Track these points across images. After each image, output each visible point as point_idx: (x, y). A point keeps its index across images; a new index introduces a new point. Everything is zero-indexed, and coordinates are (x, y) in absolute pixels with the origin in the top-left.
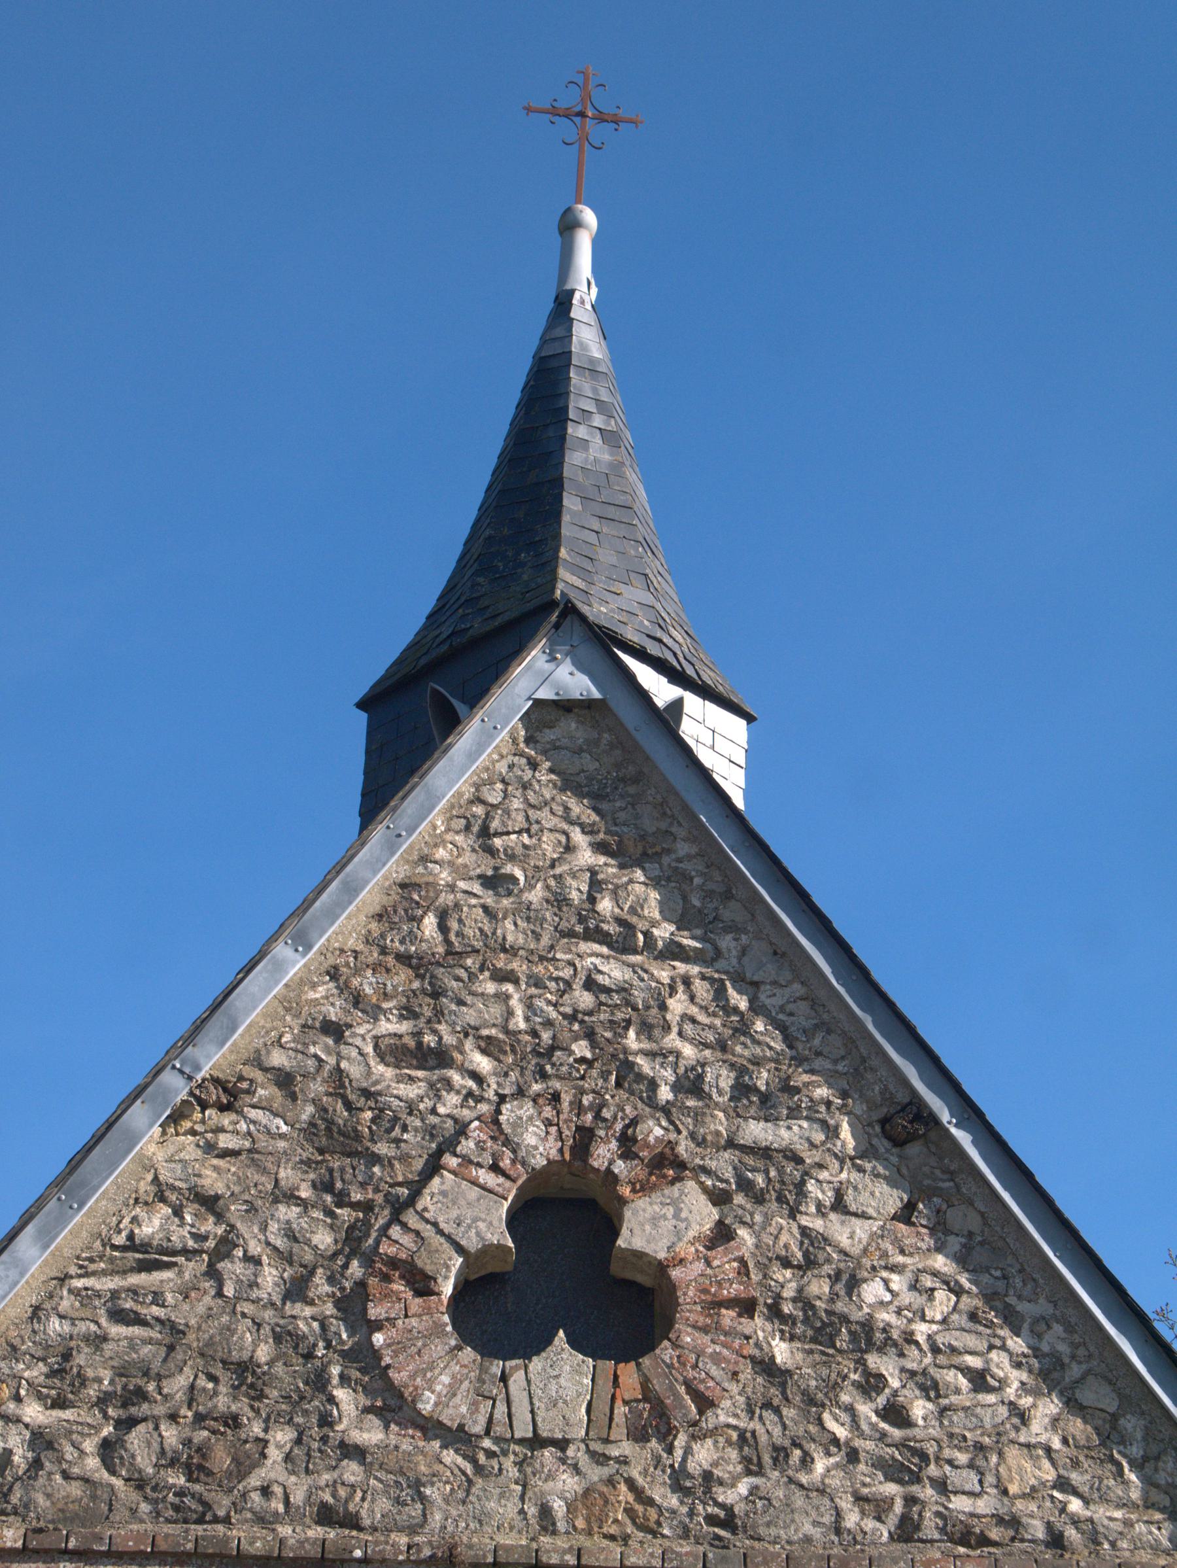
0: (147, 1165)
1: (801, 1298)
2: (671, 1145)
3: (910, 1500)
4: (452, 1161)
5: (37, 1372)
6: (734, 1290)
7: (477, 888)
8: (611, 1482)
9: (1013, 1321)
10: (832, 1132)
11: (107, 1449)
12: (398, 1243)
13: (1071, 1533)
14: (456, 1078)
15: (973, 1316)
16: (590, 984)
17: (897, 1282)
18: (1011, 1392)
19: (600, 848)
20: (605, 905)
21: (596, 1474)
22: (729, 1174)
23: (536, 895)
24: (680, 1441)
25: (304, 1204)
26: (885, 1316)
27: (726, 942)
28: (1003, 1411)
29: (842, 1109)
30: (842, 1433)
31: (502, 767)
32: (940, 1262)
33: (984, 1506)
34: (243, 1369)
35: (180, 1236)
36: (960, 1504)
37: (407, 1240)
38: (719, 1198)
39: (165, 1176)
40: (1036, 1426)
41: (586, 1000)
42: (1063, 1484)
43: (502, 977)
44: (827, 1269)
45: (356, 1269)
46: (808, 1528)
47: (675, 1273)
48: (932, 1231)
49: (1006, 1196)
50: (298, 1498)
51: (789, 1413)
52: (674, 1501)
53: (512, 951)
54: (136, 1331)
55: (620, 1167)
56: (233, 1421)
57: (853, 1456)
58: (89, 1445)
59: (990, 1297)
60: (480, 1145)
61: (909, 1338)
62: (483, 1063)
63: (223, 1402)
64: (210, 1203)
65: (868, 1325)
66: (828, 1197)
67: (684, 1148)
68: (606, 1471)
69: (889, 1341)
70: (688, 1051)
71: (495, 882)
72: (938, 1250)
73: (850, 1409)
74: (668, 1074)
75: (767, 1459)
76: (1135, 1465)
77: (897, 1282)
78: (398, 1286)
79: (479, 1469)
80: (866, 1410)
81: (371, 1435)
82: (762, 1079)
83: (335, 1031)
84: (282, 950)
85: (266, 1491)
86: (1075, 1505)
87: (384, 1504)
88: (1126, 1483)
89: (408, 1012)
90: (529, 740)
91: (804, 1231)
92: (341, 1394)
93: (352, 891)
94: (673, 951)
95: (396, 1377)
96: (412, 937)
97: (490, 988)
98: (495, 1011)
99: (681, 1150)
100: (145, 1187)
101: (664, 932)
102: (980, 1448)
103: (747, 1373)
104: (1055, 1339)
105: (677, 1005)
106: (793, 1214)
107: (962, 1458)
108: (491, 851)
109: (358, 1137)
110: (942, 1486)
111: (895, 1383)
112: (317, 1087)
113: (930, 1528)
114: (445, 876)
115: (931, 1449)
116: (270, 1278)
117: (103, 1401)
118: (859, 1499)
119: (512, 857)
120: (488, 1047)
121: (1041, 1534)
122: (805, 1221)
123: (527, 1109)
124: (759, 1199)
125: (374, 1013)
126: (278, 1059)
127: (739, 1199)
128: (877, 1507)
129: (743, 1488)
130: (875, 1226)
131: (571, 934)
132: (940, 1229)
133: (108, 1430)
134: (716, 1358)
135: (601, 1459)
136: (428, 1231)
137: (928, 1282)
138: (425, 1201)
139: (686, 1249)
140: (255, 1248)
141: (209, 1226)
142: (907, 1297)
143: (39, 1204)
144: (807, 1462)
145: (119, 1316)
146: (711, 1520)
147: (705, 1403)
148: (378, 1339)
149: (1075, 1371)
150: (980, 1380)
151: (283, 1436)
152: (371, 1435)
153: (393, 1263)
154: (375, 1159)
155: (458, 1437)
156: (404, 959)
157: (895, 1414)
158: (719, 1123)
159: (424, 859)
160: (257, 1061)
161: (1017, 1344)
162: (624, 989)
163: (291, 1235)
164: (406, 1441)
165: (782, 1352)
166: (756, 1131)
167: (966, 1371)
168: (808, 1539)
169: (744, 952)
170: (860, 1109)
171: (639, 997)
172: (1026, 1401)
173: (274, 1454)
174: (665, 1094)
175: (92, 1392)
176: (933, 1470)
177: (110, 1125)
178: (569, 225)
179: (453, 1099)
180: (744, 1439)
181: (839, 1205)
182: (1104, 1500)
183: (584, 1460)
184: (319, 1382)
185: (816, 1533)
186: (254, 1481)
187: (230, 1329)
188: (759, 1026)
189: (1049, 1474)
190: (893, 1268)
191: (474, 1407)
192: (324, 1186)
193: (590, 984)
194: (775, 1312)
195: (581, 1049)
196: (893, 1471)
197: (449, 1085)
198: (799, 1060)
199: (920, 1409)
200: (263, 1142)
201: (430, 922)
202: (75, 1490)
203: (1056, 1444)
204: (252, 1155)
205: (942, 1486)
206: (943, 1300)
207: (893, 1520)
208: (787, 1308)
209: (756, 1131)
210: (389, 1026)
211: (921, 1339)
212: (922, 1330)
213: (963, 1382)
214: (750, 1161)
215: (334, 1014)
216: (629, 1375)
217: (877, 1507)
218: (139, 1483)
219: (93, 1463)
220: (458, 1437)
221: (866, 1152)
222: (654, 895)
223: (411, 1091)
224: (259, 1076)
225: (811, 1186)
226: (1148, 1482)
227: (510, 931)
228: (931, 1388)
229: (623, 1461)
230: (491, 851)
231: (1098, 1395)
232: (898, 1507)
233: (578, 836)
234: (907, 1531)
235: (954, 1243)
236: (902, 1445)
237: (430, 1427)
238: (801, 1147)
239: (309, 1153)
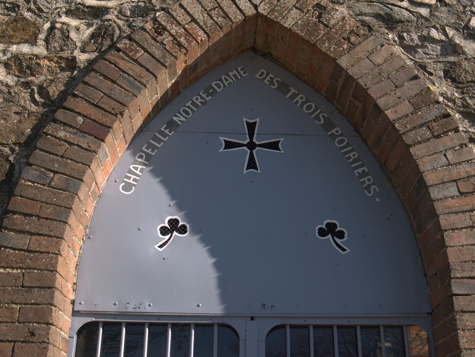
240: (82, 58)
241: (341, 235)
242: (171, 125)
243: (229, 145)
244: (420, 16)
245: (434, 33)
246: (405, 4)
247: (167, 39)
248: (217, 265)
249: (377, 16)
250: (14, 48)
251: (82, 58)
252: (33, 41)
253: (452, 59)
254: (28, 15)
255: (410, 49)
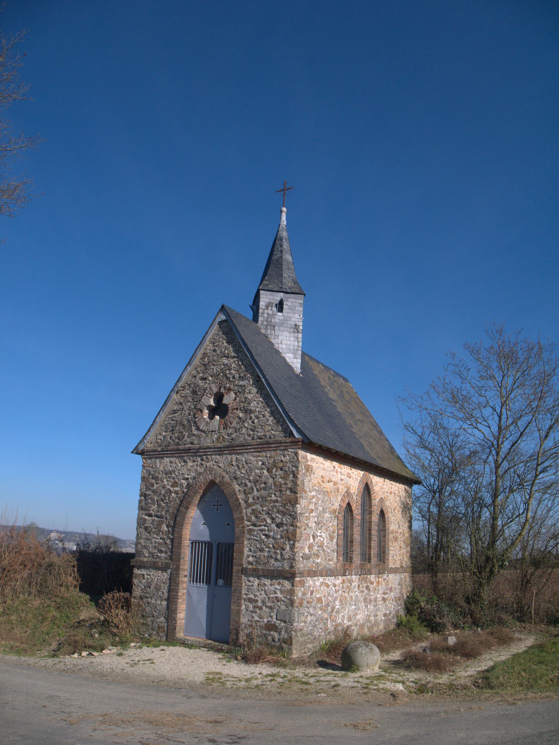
0: (175, 400)
1: (244, 407)
2: (230, 387)
3: (254, 434)
4: (205, 394)
5: (164, 428)
6: (235, 407)
7: (212, 352)
8: (220, 436)
9: (268, 406)
10: (249, 381)
11: (171, 437)
12: (199, 406)
13: (272, 436)
14: (207, 381)
15: (264, 407)
16: (224, 364)
17: (255, 403)
18: (267, 417)
19: (227, 342)
20: (226, 352)
21: (219, 435)
22: (237, 390)
23: (218, 352)
24: (228, 429)
25: (190, 402)
26: (253, 408)
27: (240, 354)
28: (266, 420)
29: (251, 378)
30: (246, 425)
31: (216, 333)
32: (261, 399)
33: (262, 434)
34: (183, 425)
35: (178, 409)
36: (259, 434)
37: (200, 406)
38: (236, 394)
39: (177, 401)
40: (269, 422)
41: (223, 366)
42: (272, 430)
43: (214, 365)
44: (247, 402)
45: (195, 410)
46: (242, 439)
47: (229, 406)
48: (260, 394)
49: (268, 388)
50: (188, 441)
51: (241, 423)
52: (227, 437)
53: (215, 361)
54: (174, 422)
55: (224, 391)
56: (182, 432)
57: (248, 429)
58: (169, 437)
59: (266, 403)
60: (208, 391)
61: (256, 411)
62: (210, 378)
63: (181, 430)
64: (181, 403)
65: (251, 410)
66: (248, 391)
67: (232, 387)
68: (219, 434)
69: (253, 412)
70: (234, 372)
71: (214, 351)
72: (261, 397)
73: (248, 422)
74: (231, 376)
75: (238, 430)
76: (281, 426)
77: (255, 403)
78: (199, 412)
79: (207, 436)
80: (250, 422)
81: (196, 432)
82: (242, 375)
83: (195, 377)
84: (188, 367)
85: (185, 441)
86: (273, 432)
87: (197, 441)
88: (279, 428)
89: (203, 373)
90: (220, 327)
91: (245, 397)
92: (193, 427)
93: (196, 357)
94: (234, 357)
95: (198, 424)
96: (204, 361)
97: (212, 367)
98: (212, 370)
99: (231, 387)
100: (175, 403)
101: (233, 354)
102: (262, 426)
103: (237, 419)
104: (274, 409)
105: (233, 365)
106: (244, 394)
107: (260, 427)
108: (214, 346)
109: (196, 392)
110: (257, 432)
111: (253, 418)
112: (192, 386)
113: (255, 437)
114: (208, 351)
115: (256, 426)
116: (187, 412)
117: (170, 431)
118: (248, 435)
119: (217, 346)
120: (212, 376)
121: (269, 437)
122: (245, 395)
123: (214, 385)
124: (240, 393)
125: (199, 373)
126: (189, 382)
127: (238, 394)
128: (249, 435)
129: (235, 435)
130: (253, 395)
131: (222, 357)
132: (261, 394)
133: (171, 435)
134: (233, 417)
135: (219, 433)
136: (202, 404)
137: (259, 402)
138: (202, 400)
139: (230, 402)
140: (185, 409)
141: (182, 407)
142: (256, 405)
143: (162, 407)
144: (242, 430)
145: (172, 420)
146: (231, 439)
147: (231, 424)
148: (196, 420)
149: (276, 412)
150: (264, 416)
151: (187, 434)
152: (196, 432)
153: (199, 409)
154: (198, 395)
155: (204, 432)
156: (203, 365)
157: (253, 422)
158: (237, 382)
159: (206, 349)
160: (186, 383)
161: (269, 410)
162: (227, 364)
163: (189, 407)
164: (199, 433)
165: (241, 415)
166: (241, 383)
167: (262, 415)
168: (241, 441)
169: (242, 355)
170: (253, 377)
171: (229, 365)
172: (268, 418)
173: (186, 436)
174: (231, 379)
175: (169, 430)
176: (256, 430)
177: (169, 395)
178: (281, 212)
179: (207, 384)
180: (235, 428)
181: (250, 393)
182: (277, 431)
183: (217, 433)
184: (191, 426)
185: (242, 440)
186: (184, 440)
187: (182, 420)
188: (242, 367)
189: (270, 428)
190: (254, 401)
191: (206, 428)
192: (193, 399)
193: (224, 364)
194: (241, 410)
195: (221, 374)
196: (253, 430)
197: (206, 382)
198: (247, 371)
199: (256, 421)
200: (187, 395)
201: (207, 358)
202: (167, 443)
203: (272, 424)
204: (186, 397)
205: (257, 432)
206: (261, 404)
207: (251, 437)
208: (242, 409)
209: (241, 383)
210: (201, 375)
211: (257, 411)
212: (257, 409)
213: (262, 416)
214: (240, 387)
215: (195, 374)
216: (223, 421)
217: (249, 435)
218: (173, 441)
219: (169, 439)
220: (204, 432)
221: (253, 384)
222: (232, 349)
223: (202, 384)
224: (187, 385)
225: (246, 390)
226: (282, 428)
227: (215, 358)
228: (257, 417)
229: (221, 433)
230: (214, 346)
231: (278, 416)
232: (252, 435)
233: (224, 341)
234: (253, 438)
235: (263, 395)
236: (253, 426)
237: (202, 431)
238: (246, 384)
239: (192, 395)
240: (185, 490)
241: (229, 525)
242: (205, 501)
243: (214, 505)
244: (242, 477)
245: (243, 481)
246: (239, 473)
247: (197, 487)
248: (210, 532)
249: (234, 477)
250: (175, 489)
251: (185, 490)
252: (177, 487)
253: (245, 488)
254: (176, 480)
255: (239, 485)
